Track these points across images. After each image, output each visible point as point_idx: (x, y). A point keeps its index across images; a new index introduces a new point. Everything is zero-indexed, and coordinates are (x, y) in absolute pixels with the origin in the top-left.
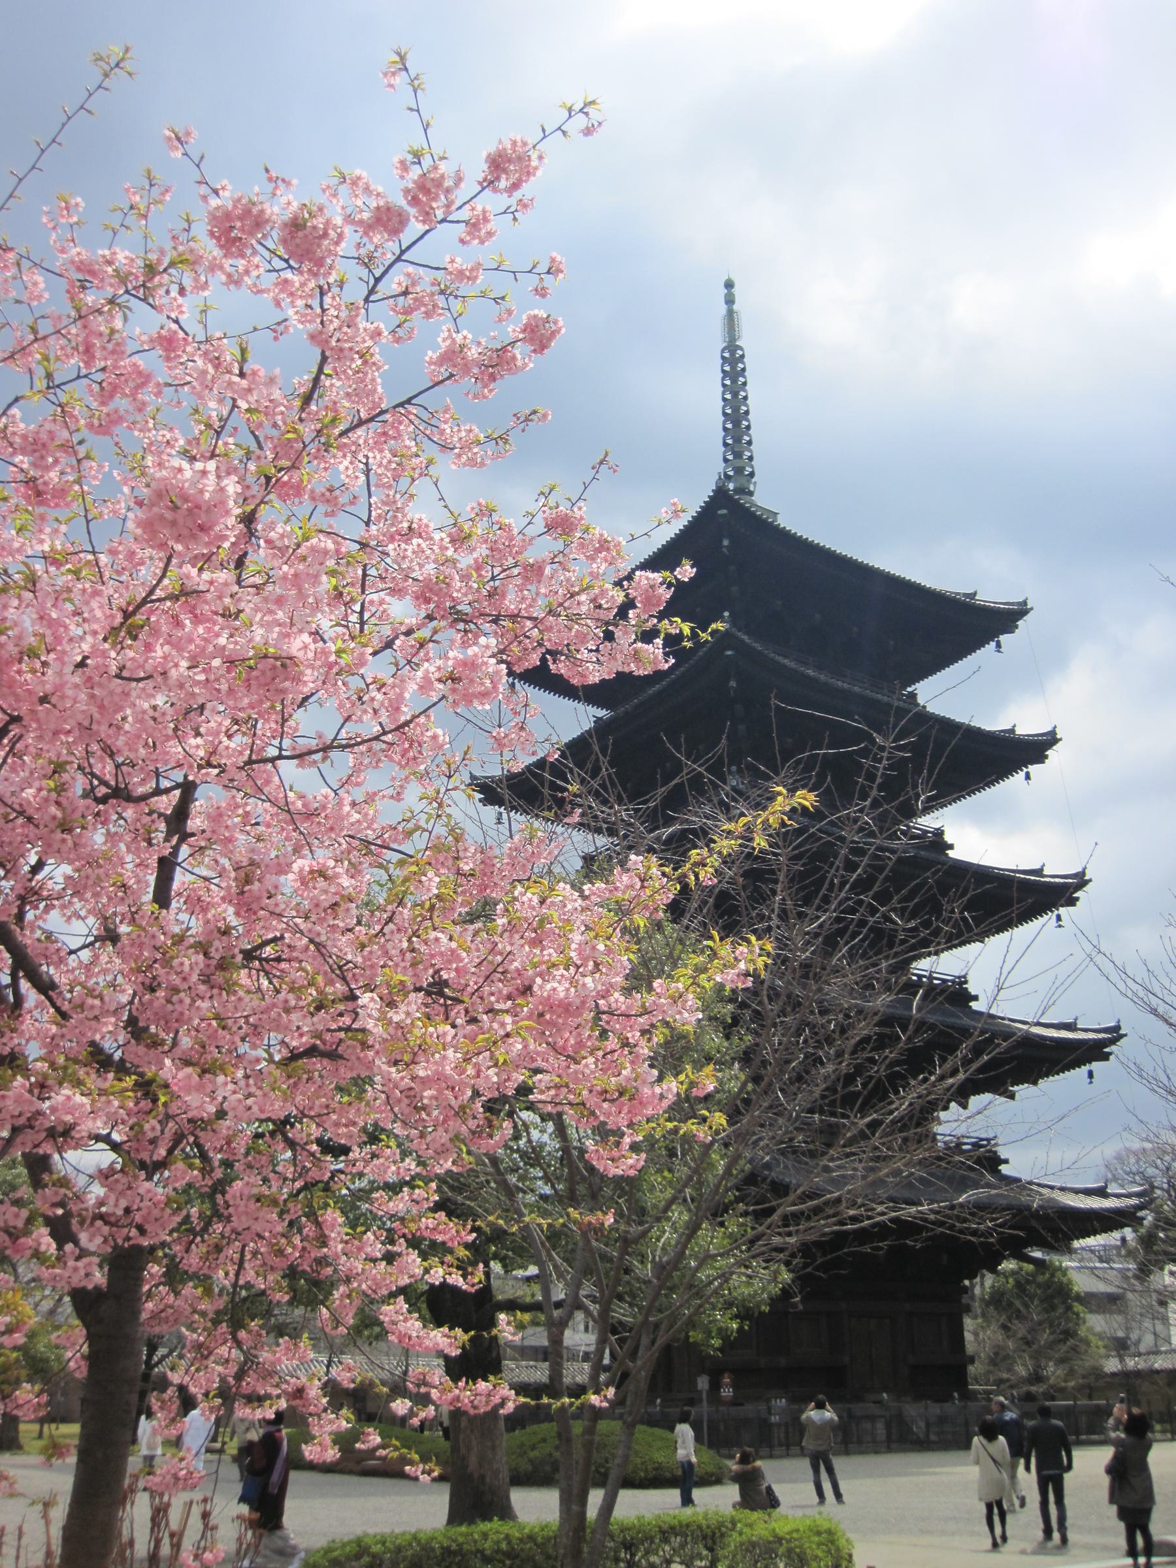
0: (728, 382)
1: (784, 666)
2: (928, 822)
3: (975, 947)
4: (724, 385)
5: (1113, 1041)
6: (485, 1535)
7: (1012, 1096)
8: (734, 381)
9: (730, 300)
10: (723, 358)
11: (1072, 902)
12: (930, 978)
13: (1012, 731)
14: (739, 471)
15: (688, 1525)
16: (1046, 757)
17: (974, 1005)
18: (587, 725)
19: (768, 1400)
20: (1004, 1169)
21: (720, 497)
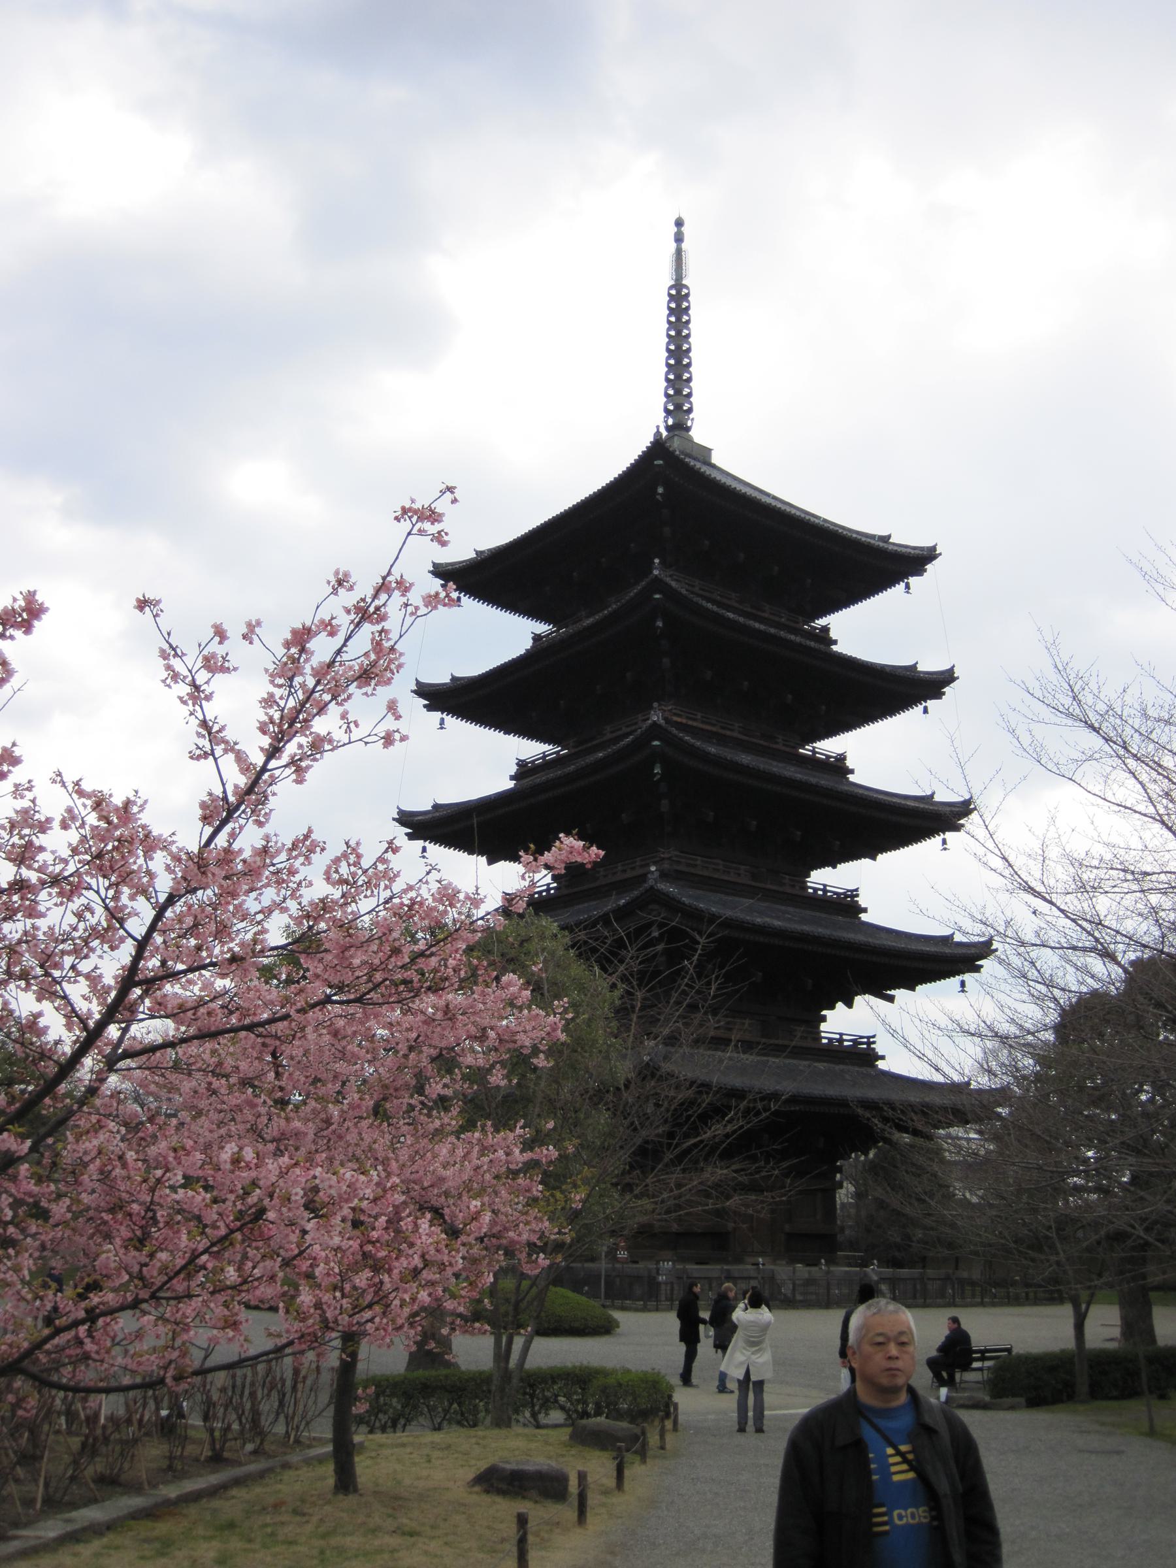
0: (673, 319)
1: (708, 609)
2: (829, 746)
3: (866, 862)
4: (669, 322)
6: (446, 1376)
7: (891, 999)
8: (679, 319)
9: (679, 239)
10: (670, 295)
11: (957, 828)
12: (825, 891)
13: (915, 666)
14: (678, 407)
15: (568, 1374)
16: (944, 693)
18: (528, 644)
19: (658, 1262)
20: (881, 1065)
21: (658, 448)
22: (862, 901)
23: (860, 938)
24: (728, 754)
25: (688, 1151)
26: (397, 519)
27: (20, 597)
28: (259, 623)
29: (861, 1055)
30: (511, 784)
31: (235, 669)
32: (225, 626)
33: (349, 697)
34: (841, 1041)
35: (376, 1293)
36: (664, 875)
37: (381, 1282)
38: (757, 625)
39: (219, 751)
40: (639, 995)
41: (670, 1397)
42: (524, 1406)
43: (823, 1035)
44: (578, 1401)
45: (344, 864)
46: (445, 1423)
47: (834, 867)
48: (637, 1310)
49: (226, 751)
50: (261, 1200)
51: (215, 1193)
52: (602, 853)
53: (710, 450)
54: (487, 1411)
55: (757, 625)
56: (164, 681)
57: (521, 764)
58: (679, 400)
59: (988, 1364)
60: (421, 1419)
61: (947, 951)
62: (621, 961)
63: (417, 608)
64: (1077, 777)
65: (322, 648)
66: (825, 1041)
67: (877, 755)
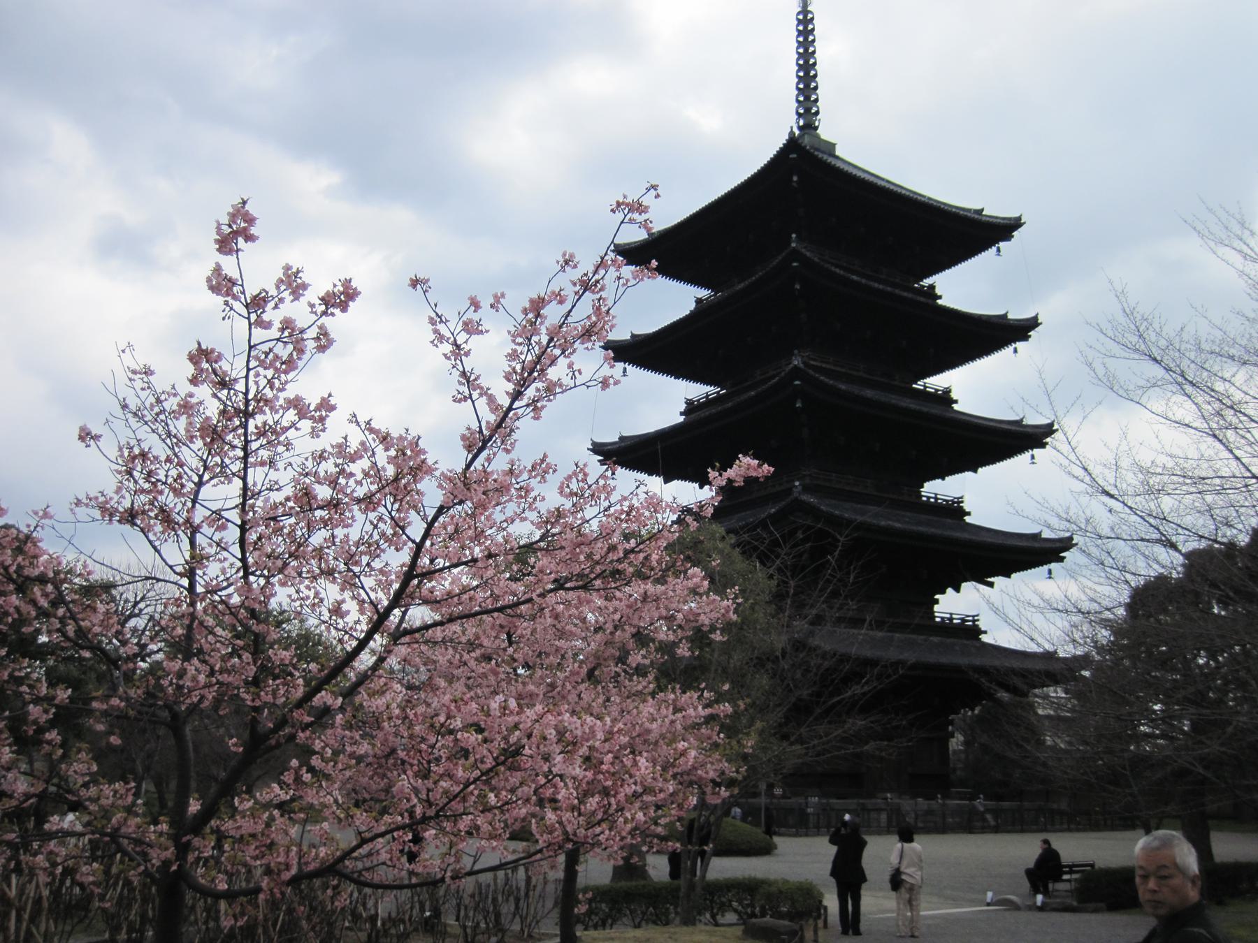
2: (936, 382)
5: (1067, 549)
6: (644, 886)
7: (991, 585)
8: (806, 39)
11: (1043, 445)
12: (936, 499)
13: (1005, 316)
14: (808, 110)
17: (967, 519)
18: (692, 306)
20: (984, 638)
21: (792, 144)
22: (966, 506)
23: (966, 536)
24: (855, 389)
25: (834, 706)
26: (613, 211)
27: (339, 284)
28: (503, 296)
29: (968, 631)
30: (682, 419)
31: (487, 331)
32: (478, 298)
33: (574, 351)
34: (951, 619)
35: (605, 812)
36: (806, 489)
37: (610, 804)
38: (876, 285)
39: (475, 395)
40: (792, 583)
41: (820, 902)
42: (705, 909)
44: (748, 905)
45: (574, 480)
46: (643, 923)
47: (943, 479)
48: (790, 836)
49: (481, 395)
50: (519, 740)
51: (486, 734)
52: (772, 469)
53: (834, 145)
54: (677, 913)
55: (876, 285)
56: (432, 342)
57: (689, 403)
58: (809, 104)
59: (1075, 876)
60: (625, 920)
61: (1037, 545)
62: (777, 557)
63: (627, 281)
64: (1143, 401)
65: (553, 313)
67: (974, 388)
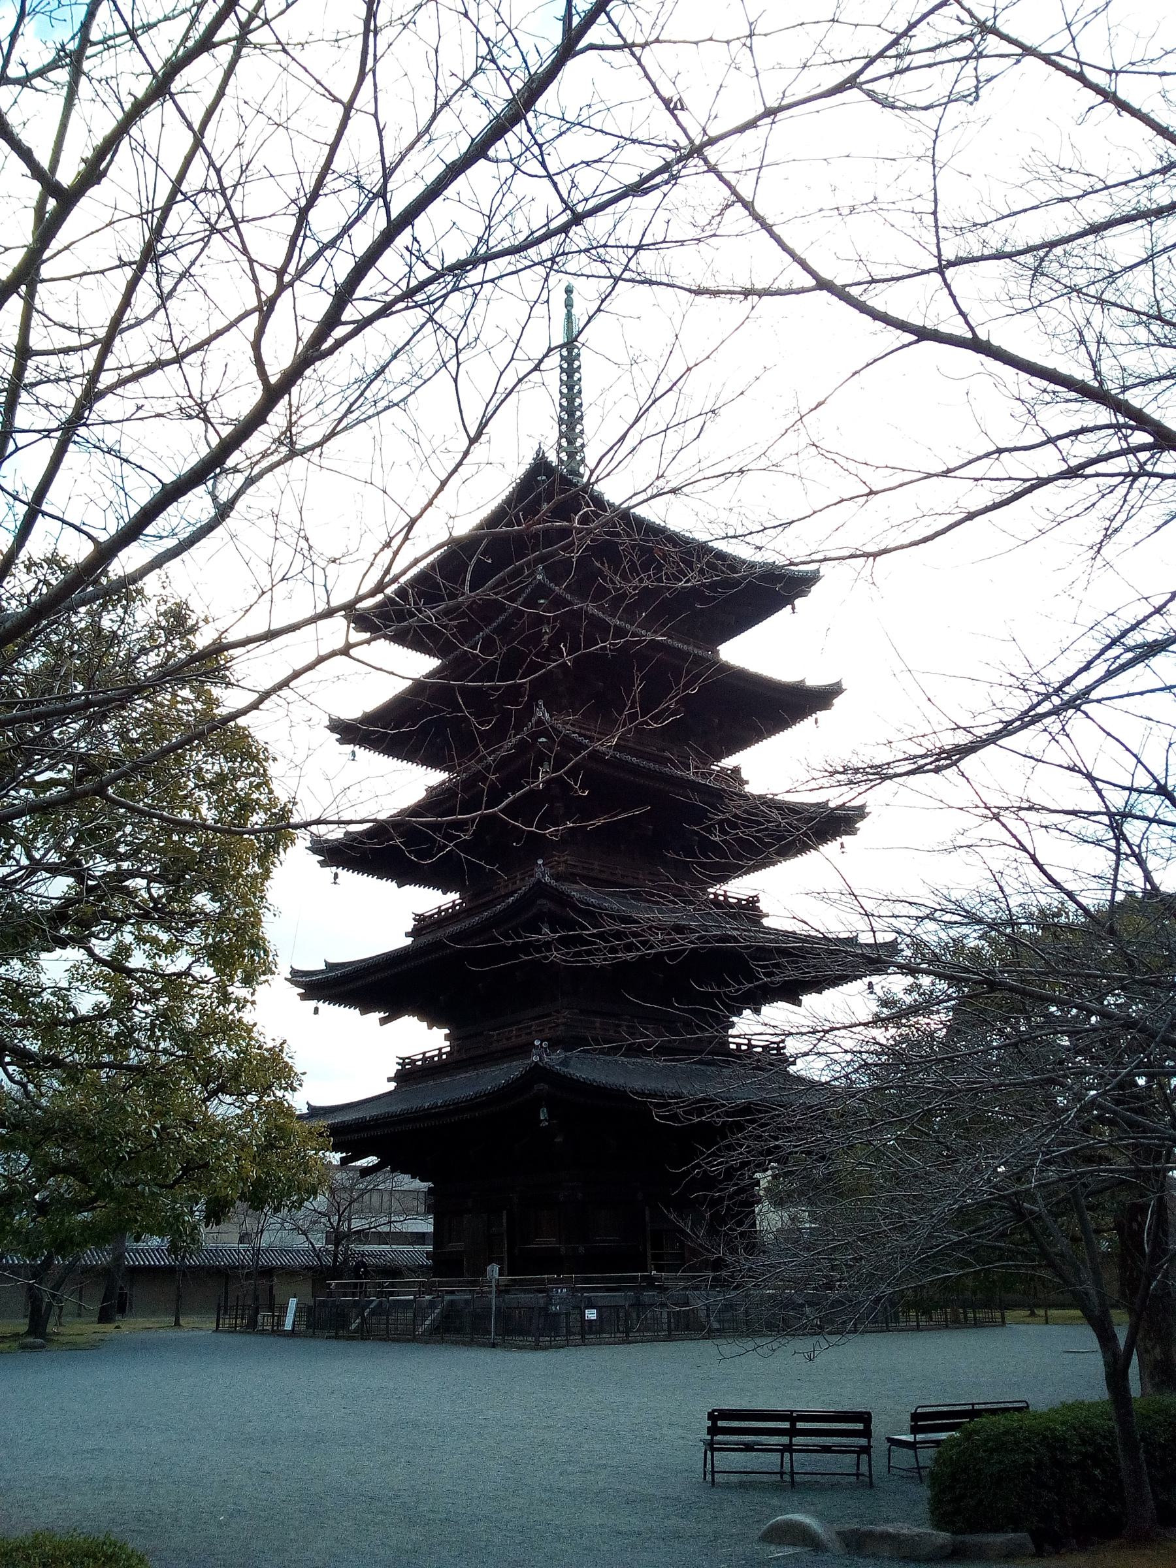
7: (798, 1003)
11: (852, 831)
12: (725, 896)
13: (803, 681)
14: (571, 455)
29: (773, 1059)
43: (731, 1040)
66: (733, 1046)
67: (769, 768)
